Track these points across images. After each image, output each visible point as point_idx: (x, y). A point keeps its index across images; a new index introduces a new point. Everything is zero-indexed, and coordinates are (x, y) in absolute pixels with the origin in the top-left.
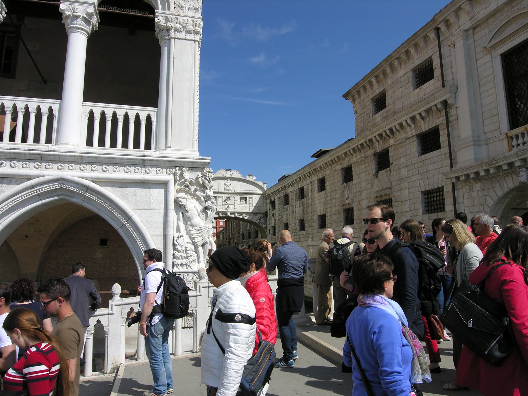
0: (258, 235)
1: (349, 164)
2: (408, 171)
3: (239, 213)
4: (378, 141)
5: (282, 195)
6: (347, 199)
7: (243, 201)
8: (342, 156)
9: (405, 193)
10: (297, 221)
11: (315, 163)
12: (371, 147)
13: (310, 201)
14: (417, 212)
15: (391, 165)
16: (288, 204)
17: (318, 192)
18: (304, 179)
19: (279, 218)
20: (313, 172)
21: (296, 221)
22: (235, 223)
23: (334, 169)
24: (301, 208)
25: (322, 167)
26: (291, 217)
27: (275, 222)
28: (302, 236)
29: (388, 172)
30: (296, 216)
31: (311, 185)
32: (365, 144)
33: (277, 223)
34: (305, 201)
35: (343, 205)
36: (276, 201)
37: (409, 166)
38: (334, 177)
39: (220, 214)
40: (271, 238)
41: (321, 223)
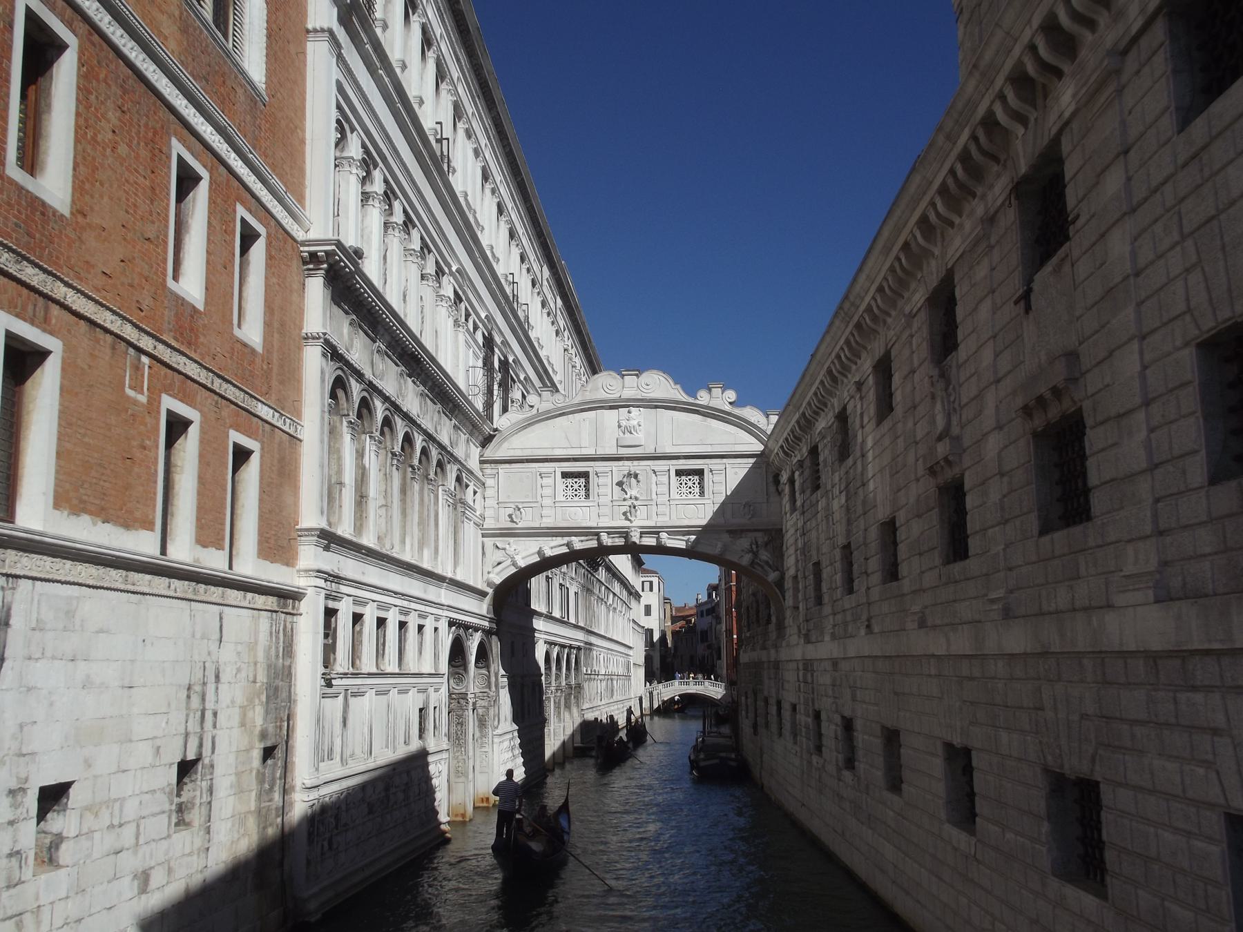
1: (944, 272)
2: (1136, 239)
4: (1022, 119)
5: (805, 451)
6: (940, 439)
7: (690, 484)
8: (915, 237)
9: (1129, 362)
10: (838, 553)
11: (852, 298)
12: (1003, 157)
14: (1184, 472)
15: (1072, 230)
16: (817, 487)
18: (846, 377)
20: (857, 342)
23: (907, 309)
26: (823, 537)
27: (797, 561)
28: (849, 618)
29: (1067, 268)
31: (861, 398)
32: (973, 149)
34: (850, 468)
35: (932, 471)
36: (797, 474)
37: (1140, 205)
38: (911, 344)
39: (604, 537)
40: (791, 624)
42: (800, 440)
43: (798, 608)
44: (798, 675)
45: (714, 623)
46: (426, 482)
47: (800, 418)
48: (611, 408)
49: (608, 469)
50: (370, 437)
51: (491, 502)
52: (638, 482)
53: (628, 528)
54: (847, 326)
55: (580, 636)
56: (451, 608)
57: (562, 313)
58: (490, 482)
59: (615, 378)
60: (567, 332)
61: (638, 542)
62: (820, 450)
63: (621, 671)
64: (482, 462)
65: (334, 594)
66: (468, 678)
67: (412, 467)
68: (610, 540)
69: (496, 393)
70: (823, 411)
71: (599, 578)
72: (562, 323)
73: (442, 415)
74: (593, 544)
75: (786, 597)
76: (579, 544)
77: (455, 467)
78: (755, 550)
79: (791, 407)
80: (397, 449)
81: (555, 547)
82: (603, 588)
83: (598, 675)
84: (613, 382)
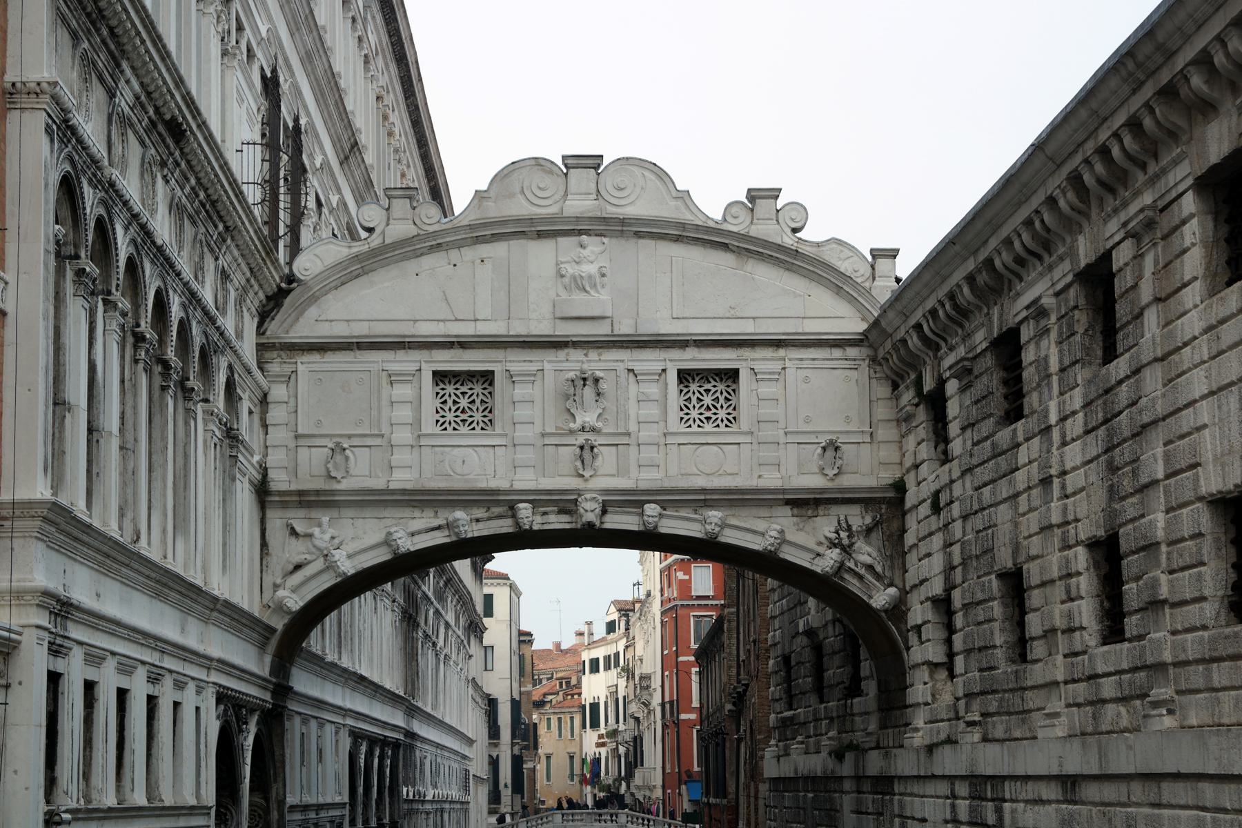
0: (862, 674)
3: (672, 499)
5: (980, 339)
7: (708, 400)
10: (1081, 558)
11: (1161, 36)
13: (1152, 380)
16: (1014, 413)
17: (1212, 292)
18: (1112, 191)
19: (969, 537)
20: (1158, 122)
21: (1070, 553)
22: (751, 581)
24: (1094, 446)
25: (1219, 59)
26: (1032, 523)
27: (950, 568)
28: (1108, 688)
30: (1065, 510)
33: (958, 575)
34: (1120, 382)
36: (952, 387)
39: (524, 510)
40: (929, 700)
41: (1233, 576)
42: (963, 313)
43: (949, 667)
44: (953, 806)
45: (622, 683)
46: (180, 394)
47: (979, 270)
48: (540, 235)
49: (533, 367)
50: (106, 302)
51: (276, 435)
52: (598, 394)
53: (579, 492)
54: (1134, 91)
55: (398, 719)
56: (225, 666)
57: (373, 18)
58: (278, 392)
59: (551, 172)
60: (380, 56)
61: (598, 524)
62: (1024, 337)
63: (454, 793)
64: (262, 348)
65: (59, 641)
66: (239, 812)
67: (166, 365)
68: (538, 519)
69: (282, 197)
70: (1039, 258)
71: (425, 588)
72: (373, 38)
73: (206, 249)
74: (503, 526)
75: (912, 637)
76: (471, 524)
77: (224, 365)
78: (846, 542)
79: (957, 248)
80: (145, 326)
81: (420, 532)
82: (431, 612)
83: (423, 802)
84: (547, 181)
